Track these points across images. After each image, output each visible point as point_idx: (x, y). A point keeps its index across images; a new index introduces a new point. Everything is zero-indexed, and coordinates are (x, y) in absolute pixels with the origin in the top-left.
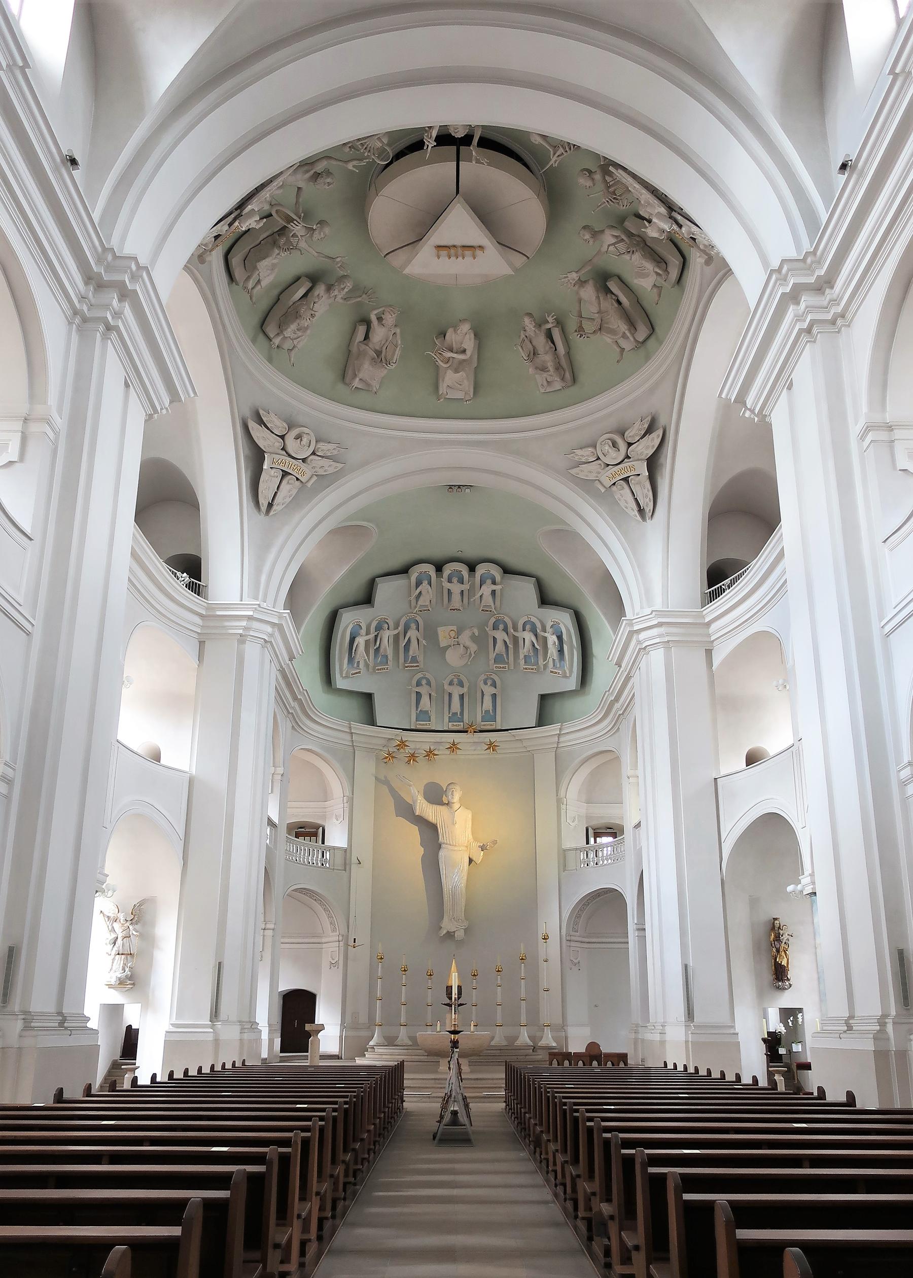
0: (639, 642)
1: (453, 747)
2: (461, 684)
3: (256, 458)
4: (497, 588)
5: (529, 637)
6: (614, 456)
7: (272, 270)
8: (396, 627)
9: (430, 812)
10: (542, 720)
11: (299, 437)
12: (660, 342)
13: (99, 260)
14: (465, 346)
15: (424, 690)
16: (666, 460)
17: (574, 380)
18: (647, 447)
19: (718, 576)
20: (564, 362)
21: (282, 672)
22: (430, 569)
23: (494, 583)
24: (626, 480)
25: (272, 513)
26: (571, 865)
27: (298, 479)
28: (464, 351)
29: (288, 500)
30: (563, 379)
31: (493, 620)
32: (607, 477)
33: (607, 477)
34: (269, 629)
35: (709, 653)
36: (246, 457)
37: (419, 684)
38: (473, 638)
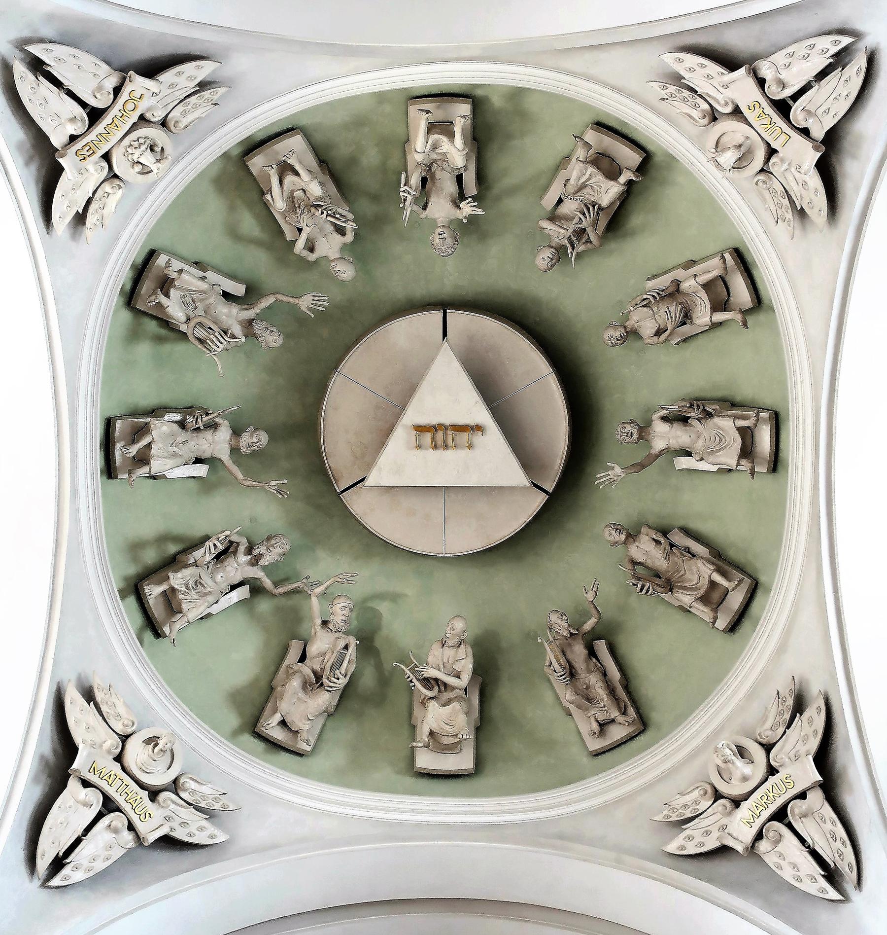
14: (458, 667)
18: (805, 740)
24: (780, 815)
25: (56, 881)
27: (131, 827)
28: (458, 677)
29: (100, 866)
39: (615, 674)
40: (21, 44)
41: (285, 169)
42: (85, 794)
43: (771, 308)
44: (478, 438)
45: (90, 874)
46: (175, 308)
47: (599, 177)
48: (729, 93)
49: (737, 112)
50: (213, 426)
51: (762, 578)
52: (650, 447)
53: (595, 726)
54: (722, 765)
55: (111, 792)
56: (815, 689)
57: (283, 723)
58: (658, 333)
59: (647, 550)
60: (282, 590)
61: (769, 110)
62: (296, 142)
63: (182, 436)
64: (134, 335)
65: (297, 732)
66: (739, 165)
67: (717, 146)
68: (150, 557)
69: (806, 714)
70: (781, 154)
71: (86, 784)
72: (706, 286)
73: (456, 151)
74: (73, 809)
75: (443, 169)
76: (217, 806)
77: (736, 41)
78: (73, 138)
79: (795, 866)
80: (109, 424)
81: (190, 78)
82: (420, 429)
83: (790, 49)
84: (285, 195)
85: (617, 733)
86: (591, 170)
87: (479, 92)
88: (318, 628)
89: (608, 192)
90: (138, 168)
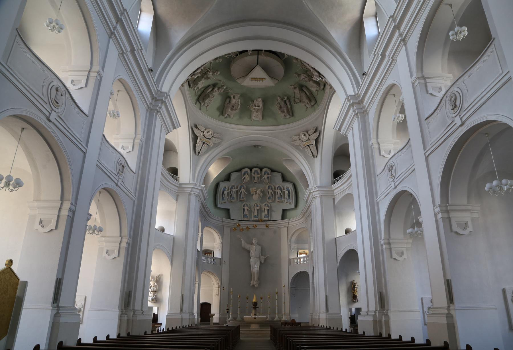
0: (313, 196)
1: (255, 226)
2: (257, 206)
3: (195, 138)
4: (269, 176)
5: (279, 191)
6: (305, 138)
7: (201, 84)
8: (237, 188)
9: (247, 247)
10: (283, 217)
11: (208, 132)
12: (318, 106)
13: (156, 94)
15: (246, 208)
17: (293, 115)
19: (337, 175)
20: (290, 110)
21: (202, 204)
22: (248, 170)
23: (268, 174)
24: (309, 146)
26: (292, 263)
28: (259, 106)
30: (289, 115)
31: (268, 186)
32: (303, 145)
33: (303, 145)
34: (198, 191)
35: (334, 199)
36: (192, 138)
37: (244, 206)
38: (262, 192)
56: (319, 129)
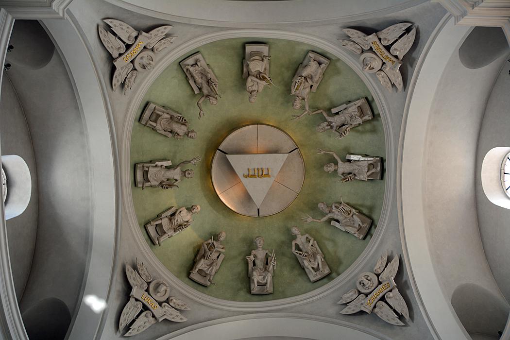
16: (104, 69)
18: (120, 74)
24: (128, 47)
25: (409, 25)
27: (380, 39)
39: (191, 82)
40: (406, 325)
41: (316, 270)
42: (397, 53)
43: (140, 225)
44: (246, 173)
45: (395, 25)
46: (357, 220)
47: (205, 269)
48: (164, 310)
49: (160, 304)
50: (343, 174)
51: (137, 123)
52: (181, 169)
53: (199, 64)
54: (151, 62)
55: (387, 53)
57: (320, 64)
58: (180, 212)
59: (181, 129)
60: (320, 111)
61: (149, 307)
62: (312, 279)
63: (356, 172)
64: (371, 209)
65: (314, 60)
66: (158, 285)
67: (166, 290)
68: (368, 127)
69: (120, 83)
70: (144, 290)
71: (396, 57)
72: (165, 233)
73: (257, 277)
74: (402, 48)
75: (260, 269)
76: (347, 42)
77: (164, 328)
78: (391, 291)
79: (122, 29)
80: (382, 178)
81: (350, 308)
82: (268, 175)
83: (145, 329)
84: (317, 260)
85: (190, 61)
86: (208, 272)
87: (249, 296)
88: (306, 97)
89: (202, 265)
90: (369, 278)
